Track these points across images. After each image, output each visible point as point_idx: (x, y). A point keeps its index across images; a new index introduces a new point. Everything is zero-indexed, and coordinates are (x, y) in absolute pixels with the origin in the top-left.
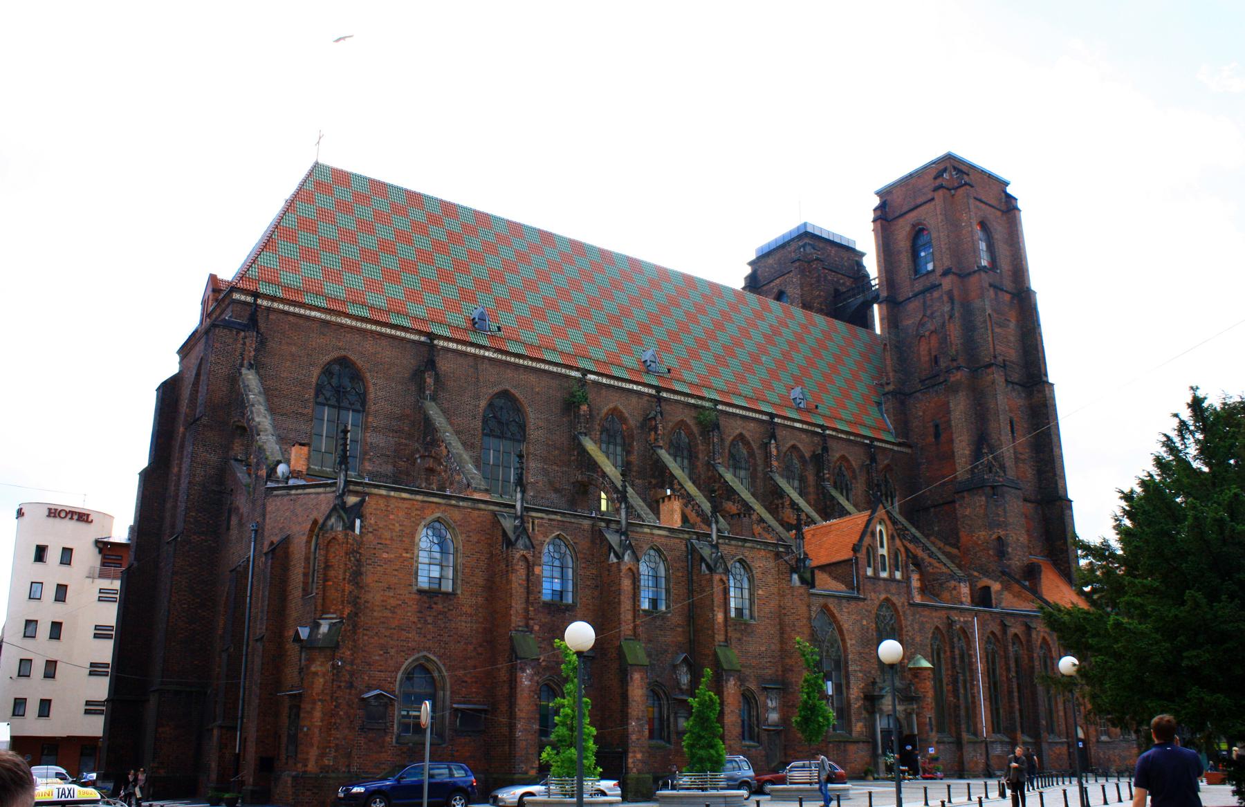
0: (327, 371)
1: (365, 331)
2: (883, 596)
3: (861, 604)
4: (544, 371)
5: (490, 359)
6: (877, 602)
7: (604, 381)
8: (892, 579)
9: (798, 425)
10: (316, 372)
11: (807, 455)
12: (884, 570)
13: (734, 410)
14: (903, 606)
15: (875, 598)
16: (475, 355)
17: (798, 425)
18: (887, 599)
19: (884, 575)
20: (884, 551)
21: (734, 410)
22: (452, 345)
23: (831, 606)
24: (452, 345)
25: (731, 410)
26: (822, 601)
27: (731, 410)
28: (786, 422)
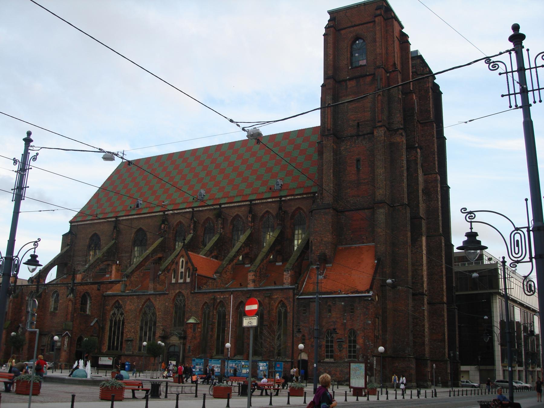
0: (91, 239)
1: (101, 222)
2: (177, 291)
3: (166, 296)
4: (154, 216)
5: (136, 218)
6: (174, 294)
7: (176, 212)
8: (185, 282)
9: (269, 200)
10: (88, 240)
11: (274, 214)
12: (181, 278)
13: (234, 205)
14: (187, 294)
15: (173, 293)
16: (131, 219)
17: (269, 200)
18: (180, 292)
19: (181, 281)
20: (183, 270)
21: (234, 205)
22: (124, 218)
23: (151, 299)
24: (124, 218)
25: (232, 205)
26: (147, 297)
27: (232, 205)
28: (262, 201)
